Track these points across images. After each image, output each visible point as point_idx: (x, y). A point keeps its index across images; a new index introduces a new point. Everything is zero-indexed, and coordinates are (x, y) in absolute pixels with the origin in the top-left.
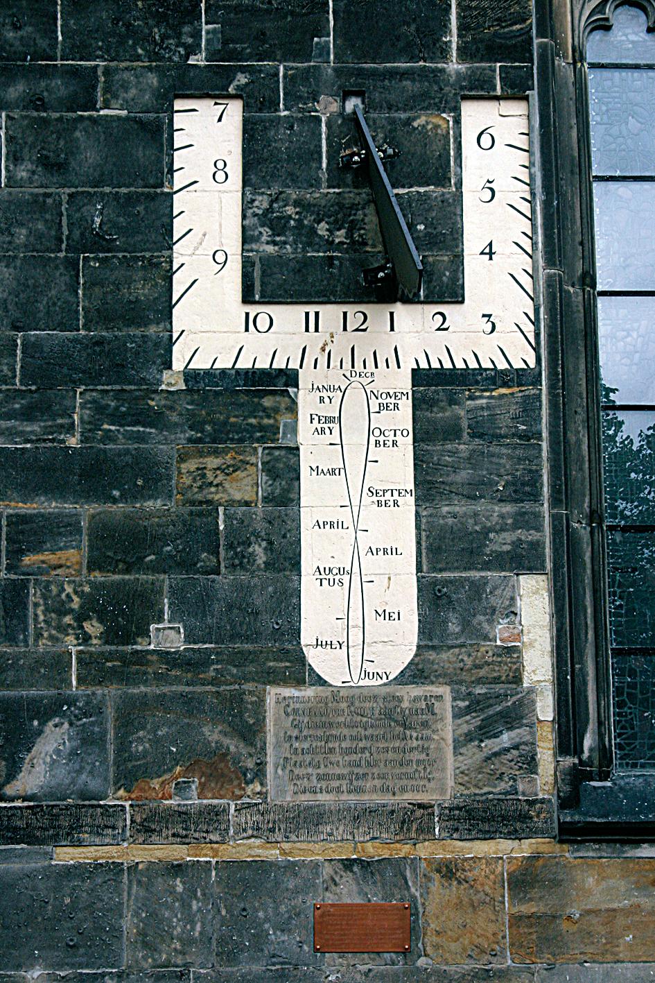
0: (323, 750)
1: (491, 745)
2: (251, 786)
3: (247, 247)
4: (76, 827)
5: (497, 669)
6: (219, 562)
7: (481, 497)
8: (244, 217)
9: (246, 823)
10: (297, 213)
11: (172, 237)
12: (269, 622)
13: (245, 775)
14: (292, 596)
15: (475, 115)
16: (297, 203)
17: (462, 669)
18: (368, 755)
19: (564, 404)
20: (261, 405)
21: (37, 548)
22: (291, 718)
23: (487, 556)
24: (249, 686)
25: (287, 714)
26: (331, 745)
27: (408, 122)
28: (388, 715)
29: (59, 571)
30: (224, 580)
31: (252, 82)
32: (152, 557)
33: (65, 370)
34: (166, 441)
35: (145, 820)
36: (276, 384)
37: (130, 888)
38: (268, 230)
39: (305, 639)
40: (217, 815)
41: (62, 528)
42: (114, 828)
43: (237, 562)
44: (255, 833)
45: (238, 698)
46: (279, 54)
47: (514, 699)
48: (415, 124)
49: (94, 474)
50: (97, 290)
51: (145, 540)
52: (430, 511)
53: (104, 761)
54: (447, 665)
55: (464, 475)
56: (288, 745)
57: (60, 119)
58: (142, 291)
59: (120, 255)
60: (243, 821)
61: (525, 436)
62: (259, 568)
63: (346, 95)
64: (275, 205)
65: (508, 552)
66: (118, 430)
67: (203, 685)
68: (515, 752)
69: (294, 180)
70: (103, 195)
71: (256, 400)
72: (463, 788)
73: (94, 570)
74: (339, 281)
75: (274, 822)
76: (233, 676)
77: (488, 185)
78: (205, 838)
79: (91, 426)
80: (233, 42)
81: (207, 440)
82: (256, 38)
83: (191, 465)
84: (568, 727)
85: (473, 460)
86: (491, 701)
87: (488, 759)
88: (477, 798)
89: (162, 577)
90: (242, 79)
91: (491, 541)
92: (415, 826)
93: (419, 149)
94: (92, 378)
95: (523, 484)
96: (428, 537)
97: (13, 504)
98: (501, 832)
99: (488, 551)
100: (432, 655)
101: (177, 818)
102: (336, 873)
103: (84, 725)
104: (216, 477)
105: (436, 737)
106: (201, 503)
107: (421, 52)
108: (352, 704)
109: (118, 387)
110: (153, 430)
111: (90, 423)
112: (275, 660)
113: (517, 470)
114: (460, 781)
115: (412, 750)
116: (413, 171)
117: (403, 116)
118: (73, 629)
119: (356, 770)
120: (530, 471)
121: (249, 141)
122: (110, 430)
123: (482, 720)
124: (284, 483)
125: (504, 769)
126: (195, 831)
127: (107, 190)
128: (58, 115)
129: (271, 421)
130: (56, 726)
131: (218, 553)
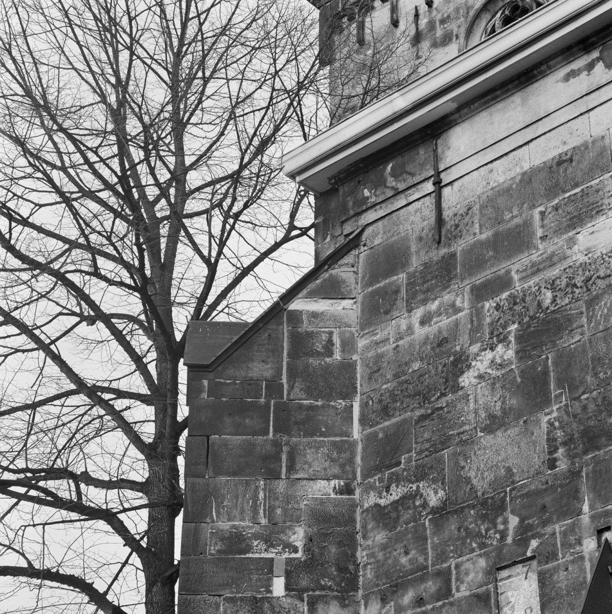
31: (541, 544)
63: (600, 532)
80: (528, 518)
90: (534, 543)
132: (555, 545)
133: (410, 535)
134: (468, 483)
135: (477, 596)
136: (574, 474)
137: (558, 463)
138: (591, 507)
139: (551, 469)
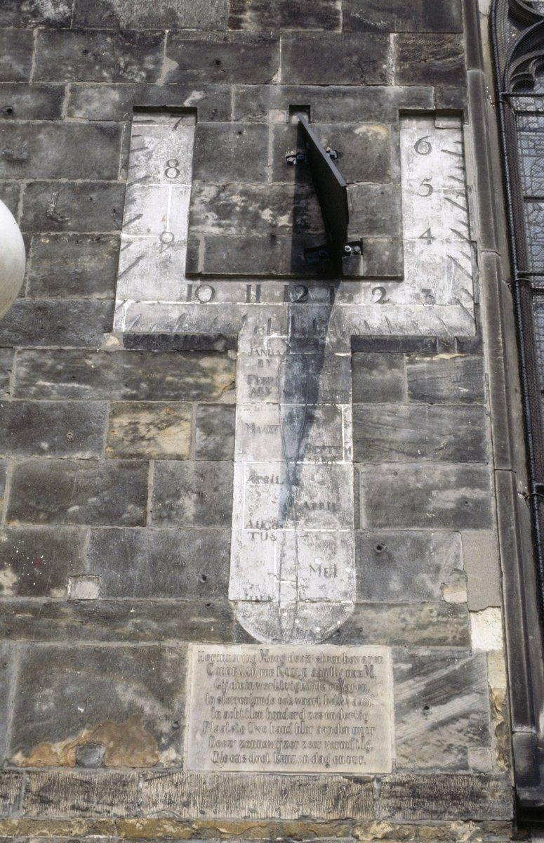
0: (248, 714)
2: (165, 753)
3: (194, 228)
5: (441, 629)
6: (146, 514)
7: (423, 454)
8: (192, 203)
9: (158, 795)
10: (243, 201)
11: (122, 219)
12: (192, 574)
13: (159, 739)
14: (221, 548)
15: (412, 131)
16: (243, 193)
17: (404, 629)
18: (299, 720)
19: (506, 371)
20: (199, 366)
22: (214, 677)
23: (430, 512)
24: (171, 643)
25: (210, 674)
26: (257, 708)
27: (350, 131)
28: (322, 677)
30: (150, 534)
31: (206, 98)
32: (76, 508)
33: (6, 332)
34: (101, 397)
35: (42, 789)
36: (212, 344)
38: (214, 214)
39: (232, 595)
40: (124, 785)
43: (165, 514)
44: (166, 807)
45: (156, 655)
46: (232, 77)
47: (462, 662)
48: (357, 132)
50: (46, 264)
52: (370, 467)
54: (387, 625)
55: (405, 434)
56: (210, 707)
57: (27, 125)
58: (89, 263)
59: (71, 234)
60: (154, 792)
61: (468, 399)
62: (187, 520)
64: (222, 195)
65: (452, 510)
66: (53, 387)
67: (120, 640)
68: (464, 723)
69: (241, 174)
70: (59, 185)
71: (194, 361)
72: (405, 760)
73: (13, 520)
74: (281, 258)
77: (425, 182)
78: (109, 812)
79: (29, 381)
80: (190, 66)
81: (142, 396)
82: (211, 65)
83: (124, 420)
84: (524, 693)
85: (412, 420)
86: (437, 664)
87: (434, 728)
88: (423, 772)
89: (83, 527)
90: (196, 95)
91: (433, 498)
92: (350, 804)
93: (359, 152)
94: (31, 338)
95: (466, 443)
96: (367, 493)
98: (450, 813)
99: (430, 507)
100: (370, 614)
101: (77, 788)
104: (148, 431)
105: (375, 702)
106: (131, 456)
107: (362, 77)
108: (283, 664)
109: (56, 347)
110: (88, 387)
111: (24, 379)
112: (200, 614)
113: (459, 430)
114: (403, 752)
115: (347, 716)
116: (353, 169)
117: (346, 125)
119: (285, 737)
120: (472, 432)
121: (200, 143)
122: (45, 387)
123: (428, 685)
124: (218, 438)
125: (452, 741)
126: (98, 803)
127: (64, 180)
128: (24, 122)
129: (208, 381)
131: (146, 504)
132: (228, 105)
133: (5, 39)
134: (108, 9)
135: (102, 130)
136: (267, 42)
137: (243, 25)
138: (285, 80)
139: (234, 28)
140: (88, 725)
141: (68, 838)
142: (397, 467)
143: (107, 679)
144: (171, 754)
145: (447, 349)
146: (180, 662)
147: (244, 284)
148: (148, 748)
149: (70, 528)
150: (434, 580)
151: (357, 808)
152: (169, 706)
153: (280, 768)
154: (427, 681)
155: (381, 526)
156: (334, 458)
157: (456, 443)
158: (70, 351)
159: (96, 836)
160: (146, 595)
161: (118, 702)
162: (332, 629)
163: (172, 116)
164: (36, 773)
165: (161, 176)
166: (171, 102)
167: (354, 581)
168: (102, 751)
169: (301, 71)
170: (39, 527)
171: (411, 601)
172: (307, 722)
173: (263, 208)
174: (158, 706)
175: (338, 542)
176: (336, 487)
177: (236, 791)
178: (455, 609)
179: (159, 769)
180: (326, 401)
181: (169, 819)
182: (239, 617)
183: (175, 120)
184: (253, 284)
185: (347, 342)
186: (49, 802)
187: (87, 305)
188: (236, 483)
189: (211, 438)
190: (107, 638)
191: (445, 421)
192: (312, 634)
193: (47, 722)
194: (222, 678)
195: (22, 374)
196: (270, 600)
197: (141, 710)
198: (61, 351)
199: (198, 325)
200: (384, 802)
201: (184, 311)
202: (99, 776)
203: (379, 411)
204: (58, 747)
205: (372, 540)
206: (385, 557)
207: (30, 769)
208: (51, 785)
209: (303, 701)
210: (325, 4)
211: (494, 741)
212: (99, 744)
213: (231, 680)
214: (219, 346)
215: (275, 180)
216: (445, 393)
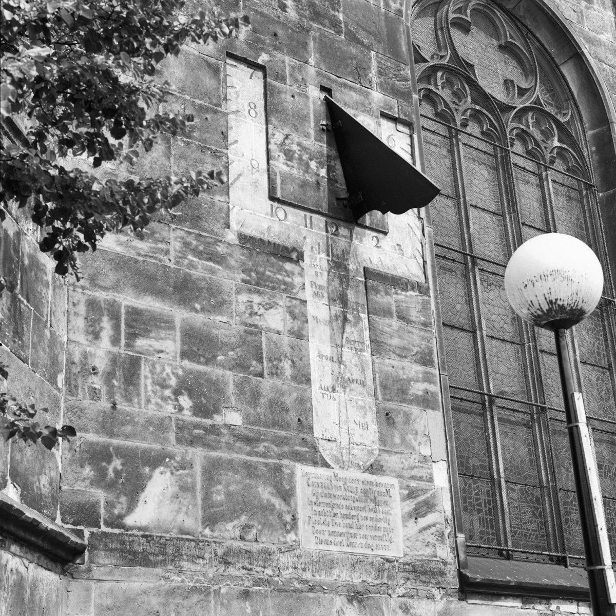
1: (423, 522)
4: (177, 555)
7: (406, 357)
13: (285, 526)
16: (299, 144)
21: (146, 333)
22: (311, 488)
24: (285, 462)
26: (335, 511)
29: (161, 355)
30: (267, 384)
37: (216, 610)
41: (166, 323)
42: (203, 558)
45: (278, 469)
49: (184, 290)
51: (217, 343)
53: (195, 505)
54: (395, 465)
55: (395, 341)
64: (286, 141)
67: (257, 456)
71: (281, 263)
75: (305, 564)
76: (275, 453)
86: (420, 492)
87: (420, 531)
88: (417, 558)
97: (128, 298)
100: (385, 456)
101: (244, 555)
102: (343, 605)
103: (180, 475)
105: (391, 512)
106: (251, 325)
109: (197, 232)
110: (220, 268)
111: (179, 252)
112: (300, 445)
118: (172, 400)
119: (351, 531)
127: (188, 97)
130: (162, 473)
132: (284, 71)
135: (209, 65)
140: (245, 513)
141: (243, 588)
142: (393, 362)
143: (253, 483)
144: (291, 537)
145: (413, 289)
146: (292, 475)
147: (302, 213)
148: (280, 532)
149: (220, 372)
150: (416, 439)
151: (389, 578)
152: (288, 504)
153: (349, 550)
154: (416, 502)
155: (388, 400)
156: (361, 350)
157: (421, 353)
158: (205, 237)
159: (258, 588)
160: (269, 427)
161: (261, 500)
162: (368, 464)
163: (248, 67)
164: (219, 543)
165: (246, 113)
166: (249, 56)
167: (377, 434)
168: (254, 531)
169: (325, 61)
170: (201, 368)
171: (405, 451)
172: (361, 522)
173: (311, 160)
174: (283, 504)
175: (367, 407)
176: (363, 370)
177: (326, 563)
178: (425, 459)
179: (287, 545)
180: (354, 309)
181: (296, 579)
182: (321, 449)
183: (251, 71)
184: (308, 214)
185: (362, 270)
186: (229, 563)
187: (213, 204)
188: (311, 357)
189: (295, 322)
190: (249, 454)
191: (415, 337)
192: (359, 466)
193: (221, 508)
194: (315, 489)
195: (177, 248)
196: (335, 441)
197: (274, 506)
198: (200, 235)
199: (279, 236)
200: (401, 574)
201: (270, 224)
202: (255, 547)
203: (383, 322)
204: (229, 526)
205: (384, 409)
206: (391, 421)
207: (215, 540)
208: (229, 552)
209: (356, 508)
210: (333, 12)
211: (447, 541)
212: (253, 526)
213: (320, 491)
214: (294, 256)
215: (316, 140)
216: (413, 318)
